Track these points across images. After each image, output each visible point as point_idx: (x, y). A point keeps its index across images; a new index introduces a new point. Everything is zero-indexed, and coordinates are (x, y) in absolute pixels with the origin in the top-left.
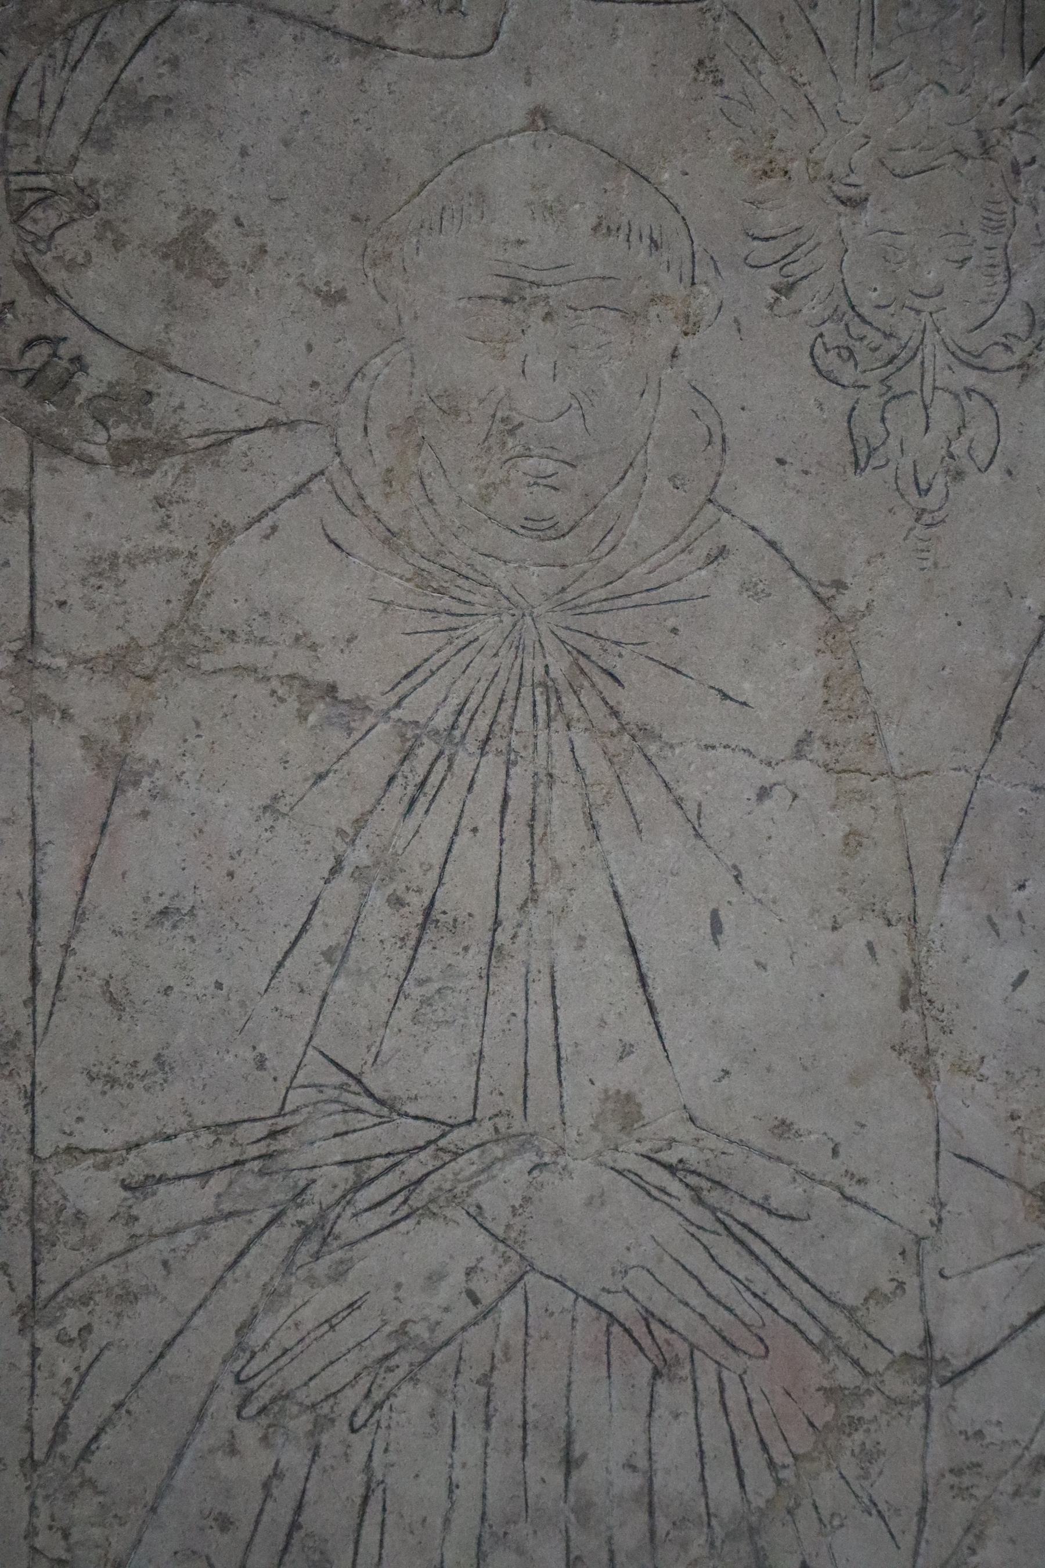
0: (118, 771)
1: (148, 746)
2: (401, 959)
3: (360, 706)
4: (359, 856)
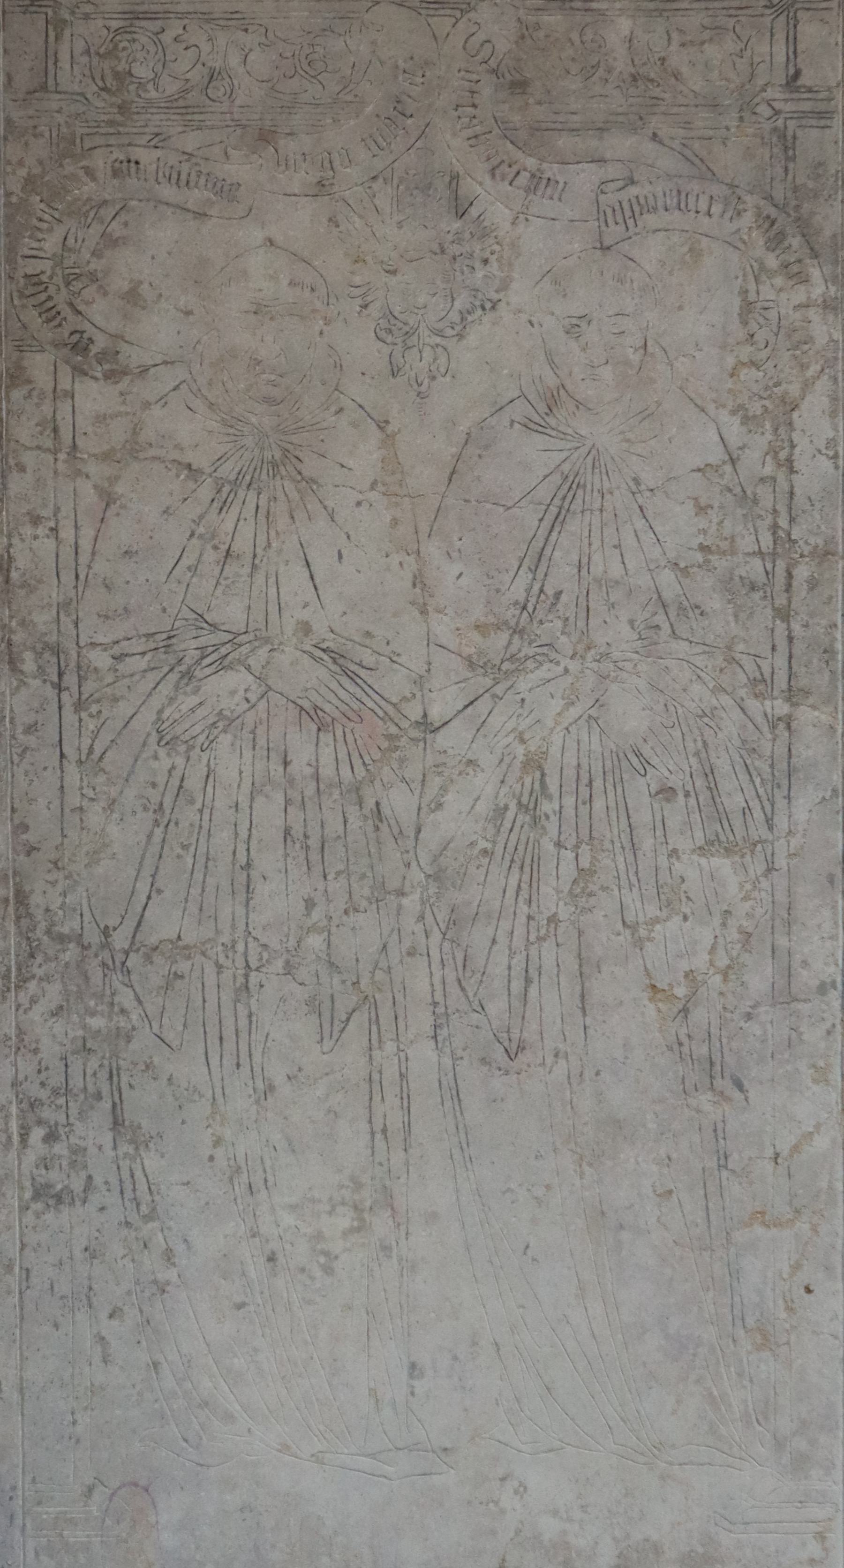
0: (108, 499)
1: (120, 489)
2: (217, 570)
3: (199, 471)
4: (201, 530)
